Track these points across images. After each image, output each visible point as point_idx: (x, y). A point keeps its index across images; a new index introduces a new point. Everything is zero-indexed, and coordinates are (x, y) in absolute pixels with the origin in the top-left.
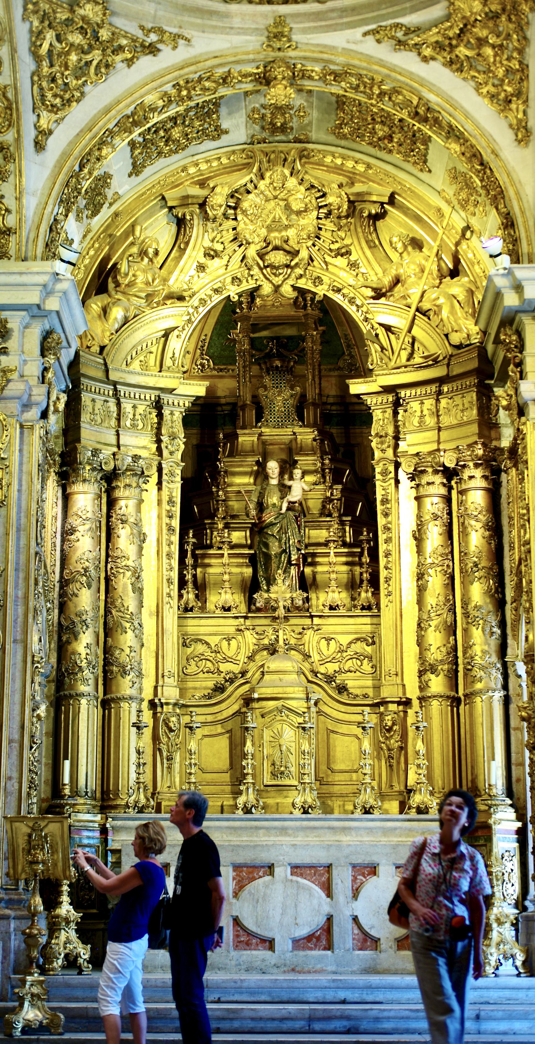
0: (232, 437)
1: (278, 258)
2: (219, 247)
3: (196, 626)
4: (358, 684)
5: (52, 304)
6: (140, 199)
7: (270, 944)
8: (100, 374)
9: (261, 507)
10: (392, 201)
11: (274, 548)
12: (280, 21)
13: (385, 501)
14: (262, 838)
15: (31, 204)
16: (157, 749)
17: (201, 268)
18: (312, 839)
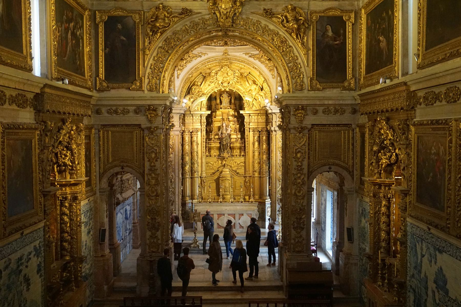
2: (213, 81)
3: (209, 159)
8: (189, 113)
9: (222, 133)
10: (249, 73)
13: (247, 136)
15: (176, 89)
17: (209, 85)
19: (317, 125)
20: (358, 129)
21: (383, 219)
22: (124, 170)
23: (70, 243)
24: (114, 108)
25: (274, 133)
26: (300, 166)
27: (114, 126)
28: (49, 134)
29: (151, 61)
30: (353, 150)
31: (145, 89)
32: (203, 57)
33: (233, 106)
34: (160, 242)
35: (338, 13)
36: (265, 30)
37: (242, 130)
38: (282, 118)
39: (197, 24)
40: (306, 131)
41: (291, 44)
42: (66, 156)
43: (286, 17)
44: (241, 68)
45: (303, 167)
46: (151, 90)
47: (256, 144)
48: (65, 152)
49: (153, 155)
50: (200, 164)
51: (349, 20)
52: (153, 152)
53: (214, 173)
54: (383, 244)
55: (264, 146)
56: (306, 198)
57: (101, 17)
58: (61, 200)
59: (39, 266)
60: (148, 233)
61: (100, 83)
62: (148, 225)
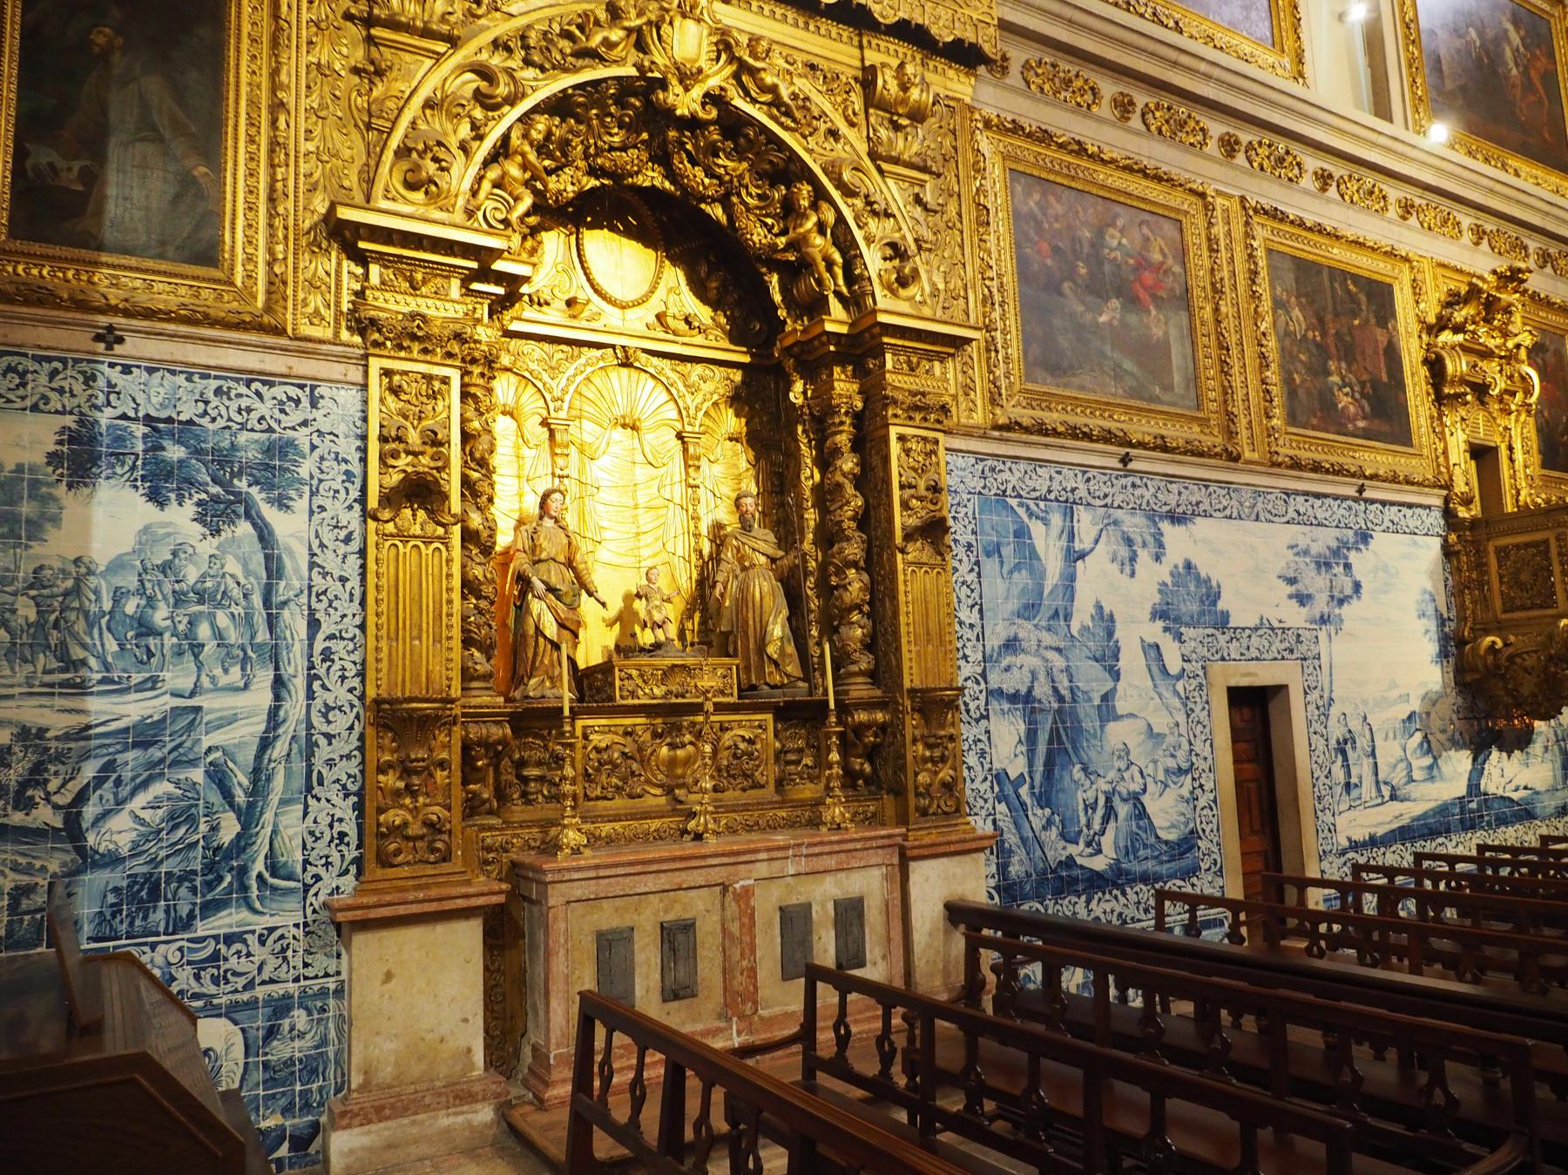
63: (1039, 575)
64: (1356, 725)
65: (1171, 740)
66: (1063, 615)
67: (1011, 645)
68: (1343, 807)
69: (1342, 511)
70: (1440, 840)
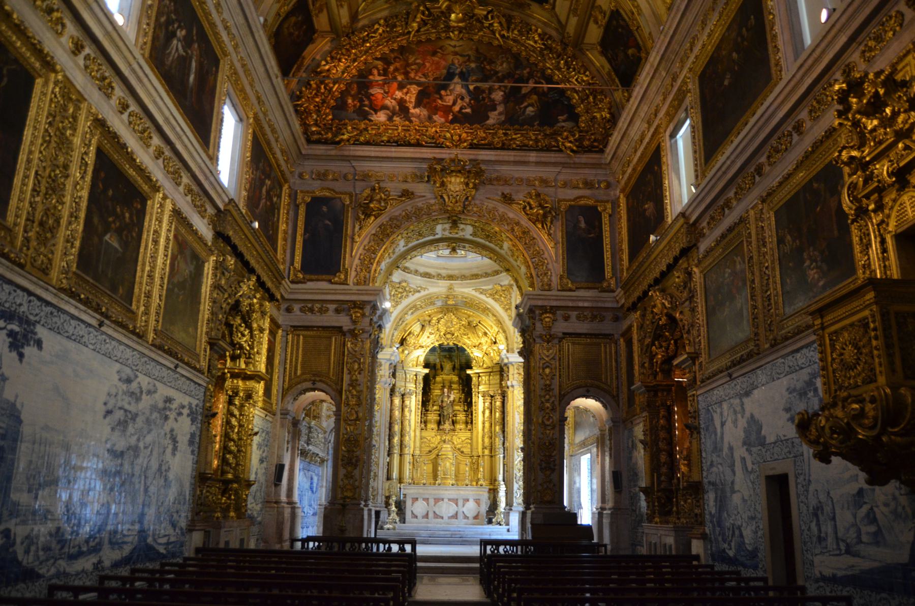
0: (434, 378)
1: (449, 336)
3: (424, 434)
4: (467, 450)
5: (393, 358)
6: (413, 320)
7: (442, 518)
9: (442, 402)
11: (445, 413)
12: (451, 284)
14: (442, 492)
16: (414, 467)
18: (453, 492)
19: (570, 334)
20: (622, 340)
21: (662, 434)
22: (315, 386)
23: (235, 457)
24: (309, 305)
25: (511, 389)
26: (550, 385)
27: (307, 328)
28: (226, 273)
29: (361, 251)
30: (617, 367)
31: (351, 284)
32: (423, 293)
33: (456, 372)
34: (357, 484)
35: (591, 202)
36: (503, 219)
37: (468, 402)
38: (524, 342)
39: (420, 209)
40: (556, 341)
41: (535, 236)
42: (243, 335)
43: (529, 203)
44: (469, 316)
45: (552, 387)
46: (358, 284)
47: (487, 412)
48: (242, 329)
49: (356, 366)
50: (412, 439)
51: (604, 210)
52: (355, 361)
53: (430, 451)
54: (664, 470)
55: (497, 414)
56: (557, 429)
57: (303, 199)
58: (230, 396)
59: (193, 435)
60: (342, 472)
61: (295, 275)
62: (342, 460)
63: (716, 435)
64: (822, 497)
65: (749, 502)
66: (721, 450)
67: (712, 465)
68: (817, 551)
69: (812, 353)
70: (884, 595)
